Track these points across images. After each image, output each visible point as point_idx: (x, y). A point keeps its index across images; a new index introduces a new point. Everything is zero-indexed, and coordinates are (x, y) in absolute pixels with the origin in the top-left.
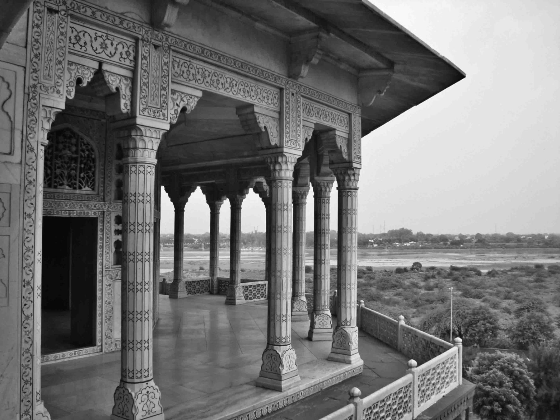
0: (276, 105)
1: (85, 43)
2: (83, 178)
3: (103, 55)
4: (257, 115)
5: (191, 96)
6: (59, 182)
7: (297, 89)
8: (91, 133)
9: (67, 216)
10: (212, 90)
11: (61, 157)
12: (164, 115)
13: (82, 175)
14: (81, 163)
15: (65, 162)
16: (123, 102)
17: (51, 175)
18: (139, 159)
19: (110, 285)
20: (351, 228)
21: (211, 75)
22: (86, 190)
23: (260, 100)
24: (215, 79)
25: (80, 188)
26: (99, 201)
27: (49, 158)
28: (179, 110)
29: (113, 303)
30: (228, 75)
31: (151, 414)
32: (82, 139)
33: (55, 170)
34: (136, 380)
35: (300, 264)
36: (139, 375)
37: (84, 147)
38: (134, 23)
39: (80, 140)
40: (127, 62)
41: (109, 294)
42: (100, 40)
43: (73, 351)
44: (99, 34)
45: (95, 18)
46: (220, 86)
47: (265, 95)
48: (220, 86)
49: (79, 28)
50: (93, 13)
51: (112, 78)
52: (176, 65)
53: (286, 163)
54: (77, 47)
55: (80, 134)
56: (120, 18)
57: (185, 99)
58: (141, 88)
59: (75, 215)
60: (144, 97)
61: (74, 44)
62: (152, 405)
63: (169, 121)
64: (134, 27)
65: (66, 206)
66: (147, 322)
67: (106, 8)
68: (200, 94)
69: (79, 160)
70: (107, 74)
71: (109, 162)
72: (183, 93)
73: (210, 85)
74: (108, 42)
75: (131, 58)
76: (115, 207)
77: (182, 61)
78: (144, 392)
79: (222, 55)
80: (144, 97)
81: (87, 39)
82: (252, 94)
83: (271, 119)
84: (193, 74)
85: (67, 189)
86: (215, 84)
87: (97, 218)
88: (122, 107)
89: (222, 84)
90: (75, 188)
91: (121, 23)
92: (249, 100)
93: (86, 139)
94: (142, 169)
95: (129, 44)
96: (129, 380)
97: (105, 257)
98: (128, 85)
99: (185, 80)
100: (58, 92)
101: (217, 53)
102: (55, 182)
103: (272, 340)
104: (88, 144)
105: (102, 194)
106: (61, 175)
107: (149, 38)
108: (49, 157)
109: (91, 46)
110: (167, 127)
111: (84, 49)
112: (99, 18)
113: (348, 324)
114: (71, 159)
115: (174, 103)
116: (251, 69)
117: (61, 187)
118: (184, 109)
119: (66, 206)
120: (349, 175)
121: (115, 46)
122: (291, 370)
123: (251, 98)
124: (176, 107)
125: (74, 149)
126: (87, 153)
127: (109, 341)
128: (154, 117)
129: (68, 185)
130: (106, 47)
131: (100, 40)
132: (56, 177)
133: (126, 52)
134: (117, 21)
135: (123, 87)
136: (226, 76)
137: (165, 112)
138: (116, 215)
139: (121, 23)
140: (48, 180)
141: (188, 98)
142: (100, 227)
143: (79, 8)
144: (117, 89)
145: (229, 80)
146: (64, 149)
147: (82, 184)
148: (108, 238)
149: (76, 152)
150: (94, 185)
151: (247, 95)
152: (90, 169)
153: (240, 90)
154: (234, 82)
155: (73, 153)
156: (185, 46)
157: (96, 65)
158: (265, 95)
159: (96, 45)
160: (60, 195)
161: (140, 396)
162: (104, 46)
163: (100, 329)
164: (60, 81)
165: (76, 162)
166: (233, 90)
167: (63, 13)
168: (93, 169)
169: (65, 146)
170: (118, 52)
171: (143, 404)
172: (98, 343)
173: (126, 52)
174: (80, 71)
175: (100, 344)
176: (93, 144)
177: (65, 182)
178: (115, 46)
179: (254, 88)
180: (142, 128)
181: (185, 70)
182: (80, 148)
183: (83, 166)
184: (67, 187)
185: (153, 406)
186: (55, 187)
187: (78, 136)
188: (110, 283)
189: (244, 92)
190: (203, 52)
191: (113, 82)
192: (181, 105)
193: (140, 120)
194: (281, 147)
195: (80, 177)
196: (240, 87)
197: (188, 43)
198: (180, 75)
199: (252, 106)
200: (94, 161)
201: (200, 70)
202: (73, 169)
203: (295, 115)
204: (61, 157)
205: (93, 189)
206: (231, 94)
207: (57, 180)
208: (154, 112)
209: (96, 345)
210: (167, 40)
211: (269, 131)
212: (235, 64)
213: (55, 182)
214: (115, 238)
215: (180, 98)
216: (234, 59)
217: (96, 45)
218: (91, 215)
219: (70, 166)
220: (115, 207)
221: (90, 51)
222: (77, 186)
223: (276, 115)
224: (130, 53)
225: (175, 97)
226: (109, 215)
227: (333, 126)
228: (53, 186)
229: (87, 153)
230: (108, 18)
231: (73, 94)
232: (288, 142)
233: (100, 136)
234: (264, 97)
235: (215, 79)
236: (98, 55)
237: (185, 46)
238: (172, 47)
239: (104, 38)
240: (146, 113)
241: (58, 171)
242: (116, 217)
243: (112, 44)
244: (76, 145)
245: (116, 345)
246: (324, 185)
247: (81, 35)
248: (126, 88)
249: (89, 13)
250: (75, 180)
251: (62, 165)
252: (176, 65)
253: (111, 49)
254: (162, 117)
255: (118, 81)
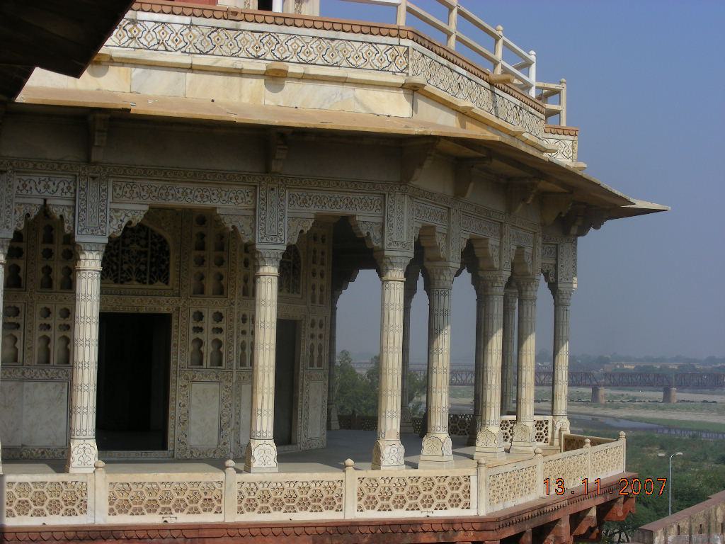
0: (249, 203)
1: (31, 188)
2: (155, 273)
3: (46, 194)
4: (222, 216)
5: (136, 211)
6: (126, 277)
7: (280, 183)
8: (163, 225)
9: (135, 311)
10: (161, 202)
11: (128, 252)
12: (102, 232)
13: (153, 269)
14: (152, 256)
15: (133, 257)
16: (66, 225)
17: (117, 270)
18: (82, 267)
19: (185, 386)
20: (387, 326)
21: (158, 190)
22: (159, 285)
23: (224, 202)
24: (164, 192)
25: (151, 283)
26: (173, 296)
27: (115, 254)
28: (124, 225)
29: (189, 406)
30: (180, 185)
31: (86, 465)
32: (152, 231)
33: (122, 265)
34: (76, 437)
35: (489, 379)
36: (78, 433)
37: (156, 240)
38: (70, 164)
39: (150, 232)
40: (68, 195)
41: (184, 395)
42: (43, 183)
43: (139, 452)
44: (43, 178)
45: (37, 169)
46: (170, 197)
47: (232, 195)
48: (170, 197)
49: (25, 178)
50: (35, 165)
51: (56, 209)
52: (118, 189)
53: (263, 259)
54: (24, 192)
55: (151, 226)
56: (58, 163)
57: (130, 214)
58: (79, 213)
59: (143, 311)
60: (82, 220)
61: (21, 191)
62: (88, 459)
63: (108, 236)
64: (72, 167)
65: (133, 301)
66: (86, 393)
67: (46, 159)
68: (146, 208)
69: (149, 254)
70: (51, 207)
71: (186, 253)
72: (127, 210)
73: (157, 198)
74: (51, 183)
75: (72, 191)
76: (192, 302)
77: (124, 184)
78: (82, 447)
79: (168, 170)
80: (82, 220)
81: (32, 184)
82: (213, 197)
83: (243, 217)
84: (137, 193)
85: (136, 285)
86: (164, 197)
87: (171, 314)
88: (66, 229)
89: (173, 195)
90: (145, 283)
91: (59, 167)
92: (208, 204)
93: (161, 232)
94: (84, 275)
95: (70, 180)
96: (72, 437)
97: (180, 357)
98: (70, 212)
99: (128, 199)
100: (8, 227)
101: (162, 170)
102: (122, 277)
103: (253, 434)
104: (161, 237)
105: (178, 288)
106: (128, 270)
107: (86, 173)
108: (115, 254)
109: (36, 189)
110: (106, 241)
111: (29, 192)
112: (40, 168)
113: (383, 436)
114: (140, 253)
115: (117, 220)
116: (208, 175)
117: (129, 283)
118: (130, 223)
119: (133, 301)
120: (385, 264)
121: (56, 184)
122: (267, 465)
123: (211, 201)
124: (120, 223)
125: (143, 242)
126: (159, 245)
127: (183, 447)
128: (92, 234)
129: (137, 280)
130: (49, 187)
131: (43, 183)
132: (123, 273)
133: (67, 188)
134: (56, 166)
135: (67, 214)
136: (178, 187)
137: (104, 229)
138: (195, 310)
139: (59, 167)
140: (114, 276)
141: (133, 213)
142: (174, 323)
143: (22, 165)
144: (61, 216)
145: (181, 190)
146: (131, 244)
147: (154, 279)
148: (183, 335)
149: (146, 246)
150: (167, 279)
151: (205, 200)
152: (163, 261)
153: (196, 197)
154: (189, 191)
155: (142, 247)
156: (125, 170)
157: (41, 202)
158: (232, 195)
159: (41, 187)
160: (127, 290)
161: (77, 449)
162: (47, 187)
163: (173, 433)
164: (9, 219)
165: (146, 256)
166: (187, 198)
167: (10, 171)
168: (167, 263)
169: (133, 241)
170: (60, 189)
171: (79, 455)
172: (170, 447)
173: (67, 188)
174: (28, 208)
175: (171, 449)
176: (167, 236)
177: (134, 278)
178: (56, 184)
179: (215, 192)
180: (82, 245)
181: (128, 190)
182: (150, 241)
183: (154, 260)
184: (135, 283)
185: (88, 459)
186: (122, 283)
187: (148, 228)
188: (185, 383)
189: (202, 198)
190: (145, 172)
191: (57, 212)
192: (126, 220)
193: (78, 239)
194: (254, 244)
195: (151, 271)
196: (197, 193)
197: (128, 168)
198: (122, 196)
199: (216, 208)
200: (168, 253)
201: (145, 188)
202: (142, 264)
203: (276, 209)
204: (128, 252)
205: (167, 284)
206: (184, 202)
207: (124, 275)
208: (92, 231)
209: (167, 449)
210: (105, 170)
211: (239, 229)
212: (185, 175)
213: (122, 277)
214: (193, 336)
215: (123, 215)
216: (184, 171)
217: (41, 187)
218: (164, 310)
219: (139, 261)
220: (192, 302)
221: (34, 192)
222: (147, 281)
223: (251, 213)
224: (71, 188)
225: (119, 214)
226: (185, 310)
227: (350, 212)
228: (119, 282)
229: (159, 245)
230: (47, 166)
231: (22, 226)
232: (262, 238)
233: (175, 227)
234: (231, 198)
235: (164, 192)
236: (43, 194)
237: (125, 170)
238: (110, 175)
239: (47, 180)
240: (84, 232)
241: (125, 267)
242: (195, 313)
243: (54, 184)
244: (146, 238)
245: (192, 452)
246: (436, 273)
247: (27, 183)
248: (69, 215)
249: (31, 165)
250: (145, 275)
251: (130, 261)
252: (118, 189)
253: (53, 188)
254: (100, 234)
255: (61, 210)
